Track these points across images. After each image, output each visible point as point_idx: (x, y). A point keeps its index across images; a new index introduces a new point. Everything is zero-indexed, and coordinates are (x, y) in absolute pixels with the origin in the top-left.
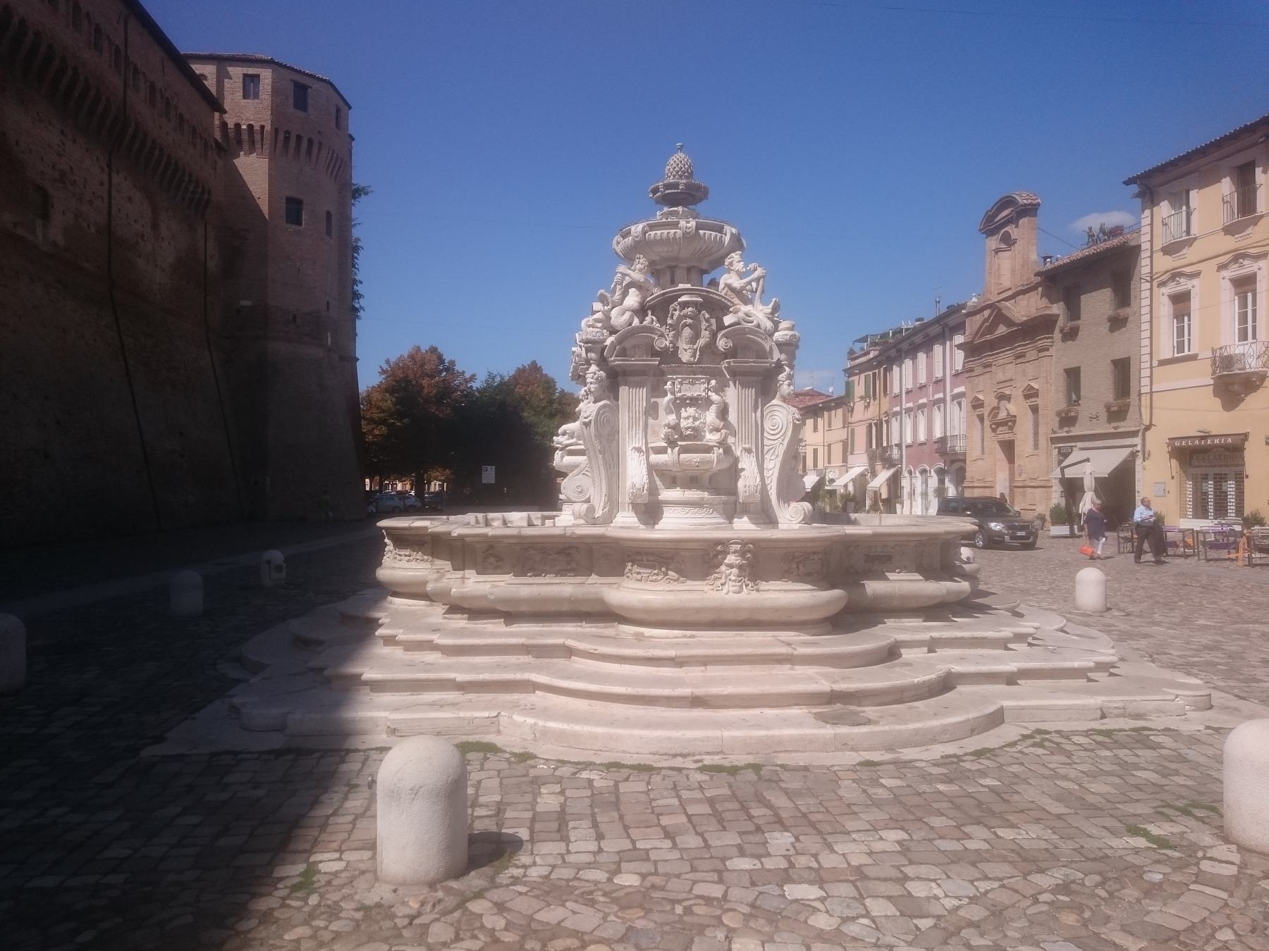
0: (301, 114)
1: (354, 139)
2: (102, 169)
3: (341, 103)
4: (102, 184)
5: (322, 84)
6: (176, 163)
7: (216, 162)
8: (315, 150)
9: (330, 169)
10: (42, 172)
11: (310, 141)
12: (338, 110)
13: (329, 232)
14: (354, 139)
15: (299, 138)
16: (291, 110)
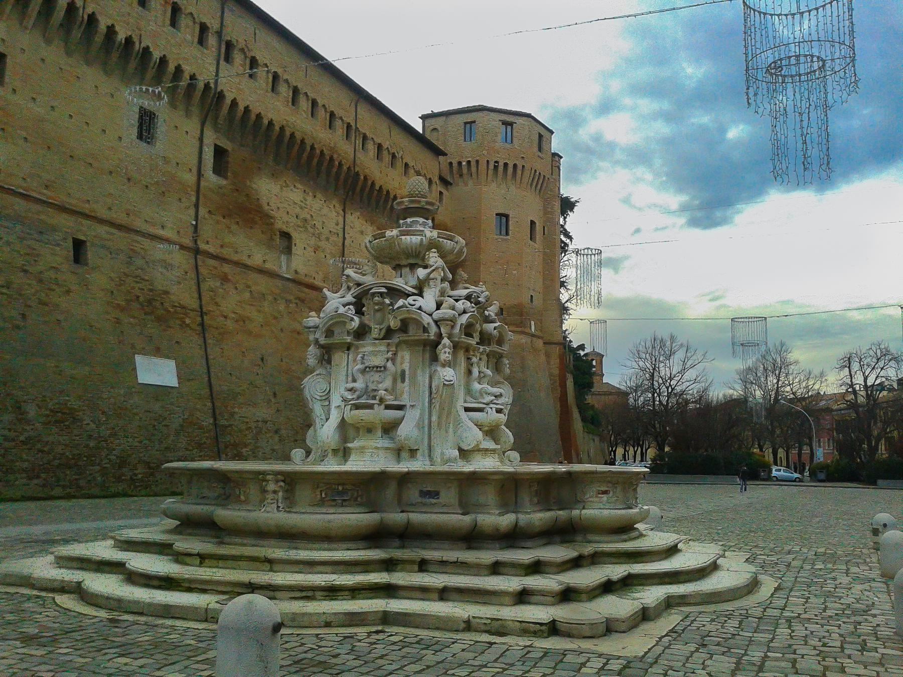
1: (561, 157)
2: (338, 214)
4: (337, 224)
7: (441, 193)
8: (519, 172)
9: (534, 184)
10: (287, 222)
11: (515, 166)
13: (532, 238)
14: (561, 157)
15: (506, 165)
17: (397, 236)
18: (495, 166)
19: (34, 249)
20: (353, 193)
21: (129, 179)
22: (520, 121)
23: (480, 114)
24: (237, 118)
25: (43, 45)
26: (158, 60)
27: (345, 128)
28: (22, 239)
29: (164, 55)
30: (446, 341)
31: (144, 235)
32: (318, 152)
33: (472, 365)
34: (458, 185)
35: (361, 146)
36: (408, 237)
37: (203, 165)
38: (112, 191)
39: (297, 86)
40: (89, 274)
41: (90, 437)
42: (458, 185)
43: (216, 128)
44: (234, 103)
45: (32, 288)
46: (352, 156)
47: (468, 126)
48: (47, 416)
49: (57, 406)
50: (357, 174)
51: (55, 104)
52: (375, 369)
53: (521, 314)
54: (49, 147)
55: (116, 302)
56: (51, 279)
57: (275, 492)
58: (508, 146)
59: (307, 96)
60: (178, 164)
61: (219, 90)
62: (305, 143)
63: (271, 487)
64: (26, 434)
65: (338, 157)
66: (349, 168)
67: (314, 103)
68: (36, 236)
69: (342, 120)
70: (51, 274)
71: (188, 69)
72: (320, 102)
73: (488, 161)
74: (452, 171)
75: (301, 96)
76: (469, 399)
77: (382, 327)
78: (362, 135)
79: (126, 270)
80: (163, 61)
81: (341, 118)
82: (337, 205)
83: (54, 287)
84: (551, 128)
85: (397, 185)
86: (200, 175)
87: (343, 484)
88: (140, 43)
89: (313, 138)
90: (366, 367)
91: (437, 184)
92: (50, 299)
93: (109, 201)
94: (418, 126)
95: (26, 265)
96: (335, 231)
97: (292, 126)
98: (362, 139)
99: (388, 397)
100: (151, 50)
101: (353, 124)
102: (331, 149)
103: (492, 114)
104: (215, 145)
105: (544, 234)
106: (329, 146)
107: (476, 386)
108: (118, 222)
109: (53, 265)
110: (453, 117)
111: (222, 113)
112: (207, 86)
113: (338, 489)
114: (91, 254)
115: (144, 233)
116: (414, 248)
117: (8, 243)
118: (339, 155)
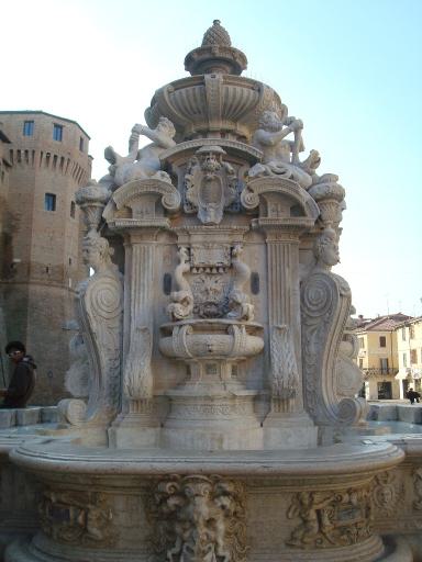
0: (58, 143)
8: (65, 163)
11: (63, 158)
12: (82, 140)
13: (72, 215)
15: (55, 156)
16: (51, 140)
22: (69, 125)
23: (38, 116)
57: (210, 522)
116: (243, 102)
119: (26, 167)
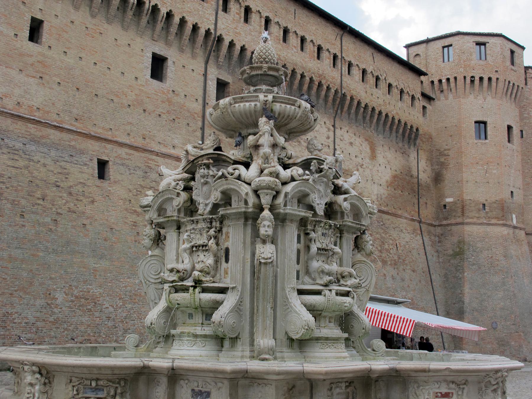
2: (329, 130)
3: (514, 48)
4: (328, 138)
5: (496, 38)
6: (387, 115)
7: (424, 108)
8: (494, 83)
9: (509, 93)
11: (490, 79)
15: (481, 79)
17: (231, 104)
18: (471, 80)
19: (65, 169)
20: (342, 111)
21: (144, 110)
23: (457, 38)
24: (235, 56)
25: (72, 11)
26: (165, 15)
27: (332, 58)
28: (56, 161)
29: (170, 11)
30: (266, 213)
31: (157, 154)
32: (307, 79)
33: (310, 240)
34: (439, 100)
35: (347, 72)
36: (242, 104)
37: (207, 96)
38: (130, 120)
39: (287, 27)
40: (110, 187)
41: (109, 318)
42: (439, 100)
43: (219, 67)
44: (232, 44)
45: (63, 199)
46: (339, 81)
47: (446, 49)
48: (72, 301)
49: (81, 293)
50: (344, 95)
51: (83, 55)
52: (201, 248)
53: (503, 209)
54: (78, 89)
55: (133, 209)
56: (78, 191)
58: (481, 62)
59: (297, 34)
60: (185, 96)
61: (218, 34)
62: (296, 72)
63: (29, 378)
64: (55, 316)
65: (326, 82)
66: (336, 91)
67: (303, 40)
68: (67, 158)
69: (329, 52)
70: (80, 188)
71: (191, 21)
72: (308, 38)
73: (465, 77)
74: (434, 88)
75: (291, 34)
76: (307, 279)
77: (207, 202)
78: (347, 63)
79: (142, 183)
80: (169, 15)
81: (328, 50)
82: (328, 122)
83: (82, 198)
84: (522, 45)
85: (382, 103)
86: (205, 104)
87: (97, 380)
88: (150, 2)
89: (303, 68)
90: (193, 247)
91: (419, 100)
92: (78, 208)
93: (128, 128)
94: (403, 54)
95: (58, 182)
96: (327, 144)
97: (283, 59)
98: (347, 66)
99: (204, 279)
100: (159, 7)
101: (339, 55)
102: (320, 76)
103: (467, 37)
104: (218, 79)
105: (522, 137)
106: (318, 74)
107: (315, 264)
108: (136, 144)
109: (81, 181)
110: (432, 43)
111: (221, 54)
112: (208, 33)
113: (91, 385)
114: (112, 170)
115: (158, 153)
117: (45, 165)
118: (327, 81)
119: (451, 96)
